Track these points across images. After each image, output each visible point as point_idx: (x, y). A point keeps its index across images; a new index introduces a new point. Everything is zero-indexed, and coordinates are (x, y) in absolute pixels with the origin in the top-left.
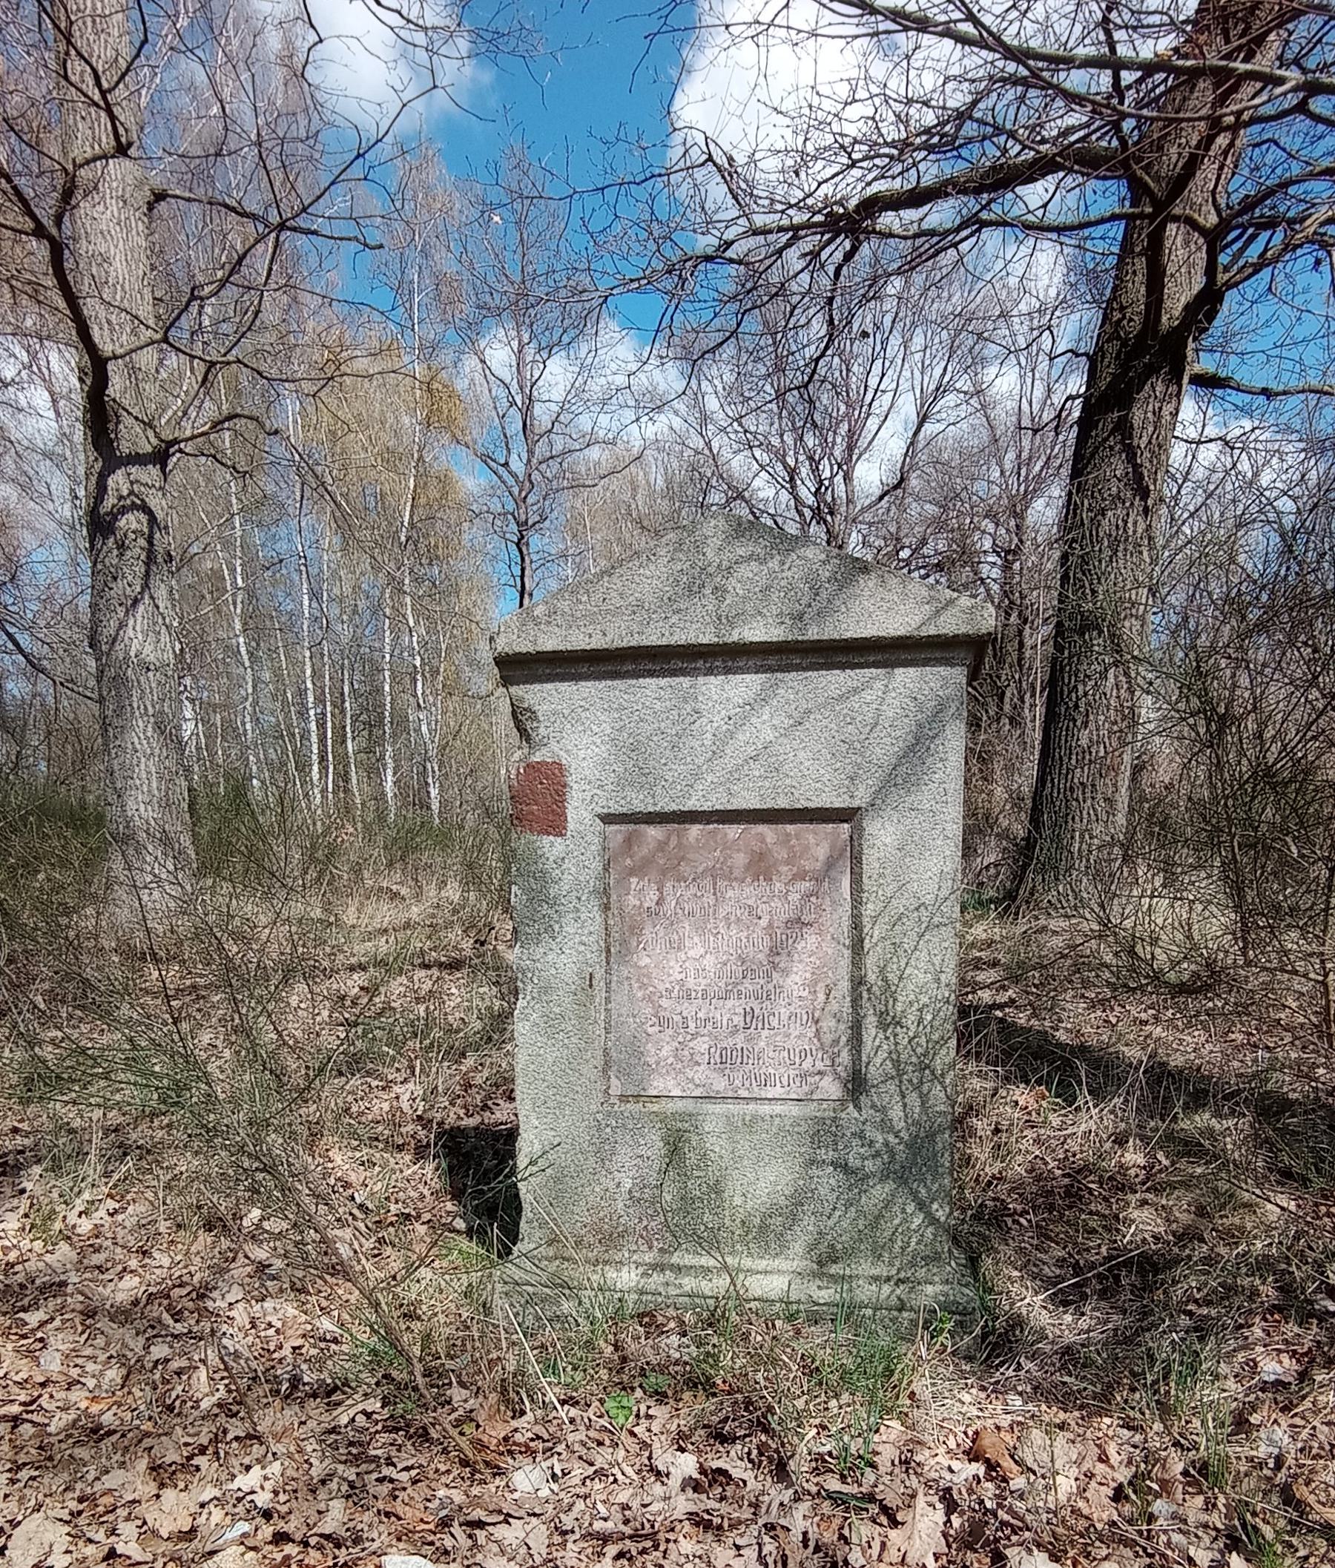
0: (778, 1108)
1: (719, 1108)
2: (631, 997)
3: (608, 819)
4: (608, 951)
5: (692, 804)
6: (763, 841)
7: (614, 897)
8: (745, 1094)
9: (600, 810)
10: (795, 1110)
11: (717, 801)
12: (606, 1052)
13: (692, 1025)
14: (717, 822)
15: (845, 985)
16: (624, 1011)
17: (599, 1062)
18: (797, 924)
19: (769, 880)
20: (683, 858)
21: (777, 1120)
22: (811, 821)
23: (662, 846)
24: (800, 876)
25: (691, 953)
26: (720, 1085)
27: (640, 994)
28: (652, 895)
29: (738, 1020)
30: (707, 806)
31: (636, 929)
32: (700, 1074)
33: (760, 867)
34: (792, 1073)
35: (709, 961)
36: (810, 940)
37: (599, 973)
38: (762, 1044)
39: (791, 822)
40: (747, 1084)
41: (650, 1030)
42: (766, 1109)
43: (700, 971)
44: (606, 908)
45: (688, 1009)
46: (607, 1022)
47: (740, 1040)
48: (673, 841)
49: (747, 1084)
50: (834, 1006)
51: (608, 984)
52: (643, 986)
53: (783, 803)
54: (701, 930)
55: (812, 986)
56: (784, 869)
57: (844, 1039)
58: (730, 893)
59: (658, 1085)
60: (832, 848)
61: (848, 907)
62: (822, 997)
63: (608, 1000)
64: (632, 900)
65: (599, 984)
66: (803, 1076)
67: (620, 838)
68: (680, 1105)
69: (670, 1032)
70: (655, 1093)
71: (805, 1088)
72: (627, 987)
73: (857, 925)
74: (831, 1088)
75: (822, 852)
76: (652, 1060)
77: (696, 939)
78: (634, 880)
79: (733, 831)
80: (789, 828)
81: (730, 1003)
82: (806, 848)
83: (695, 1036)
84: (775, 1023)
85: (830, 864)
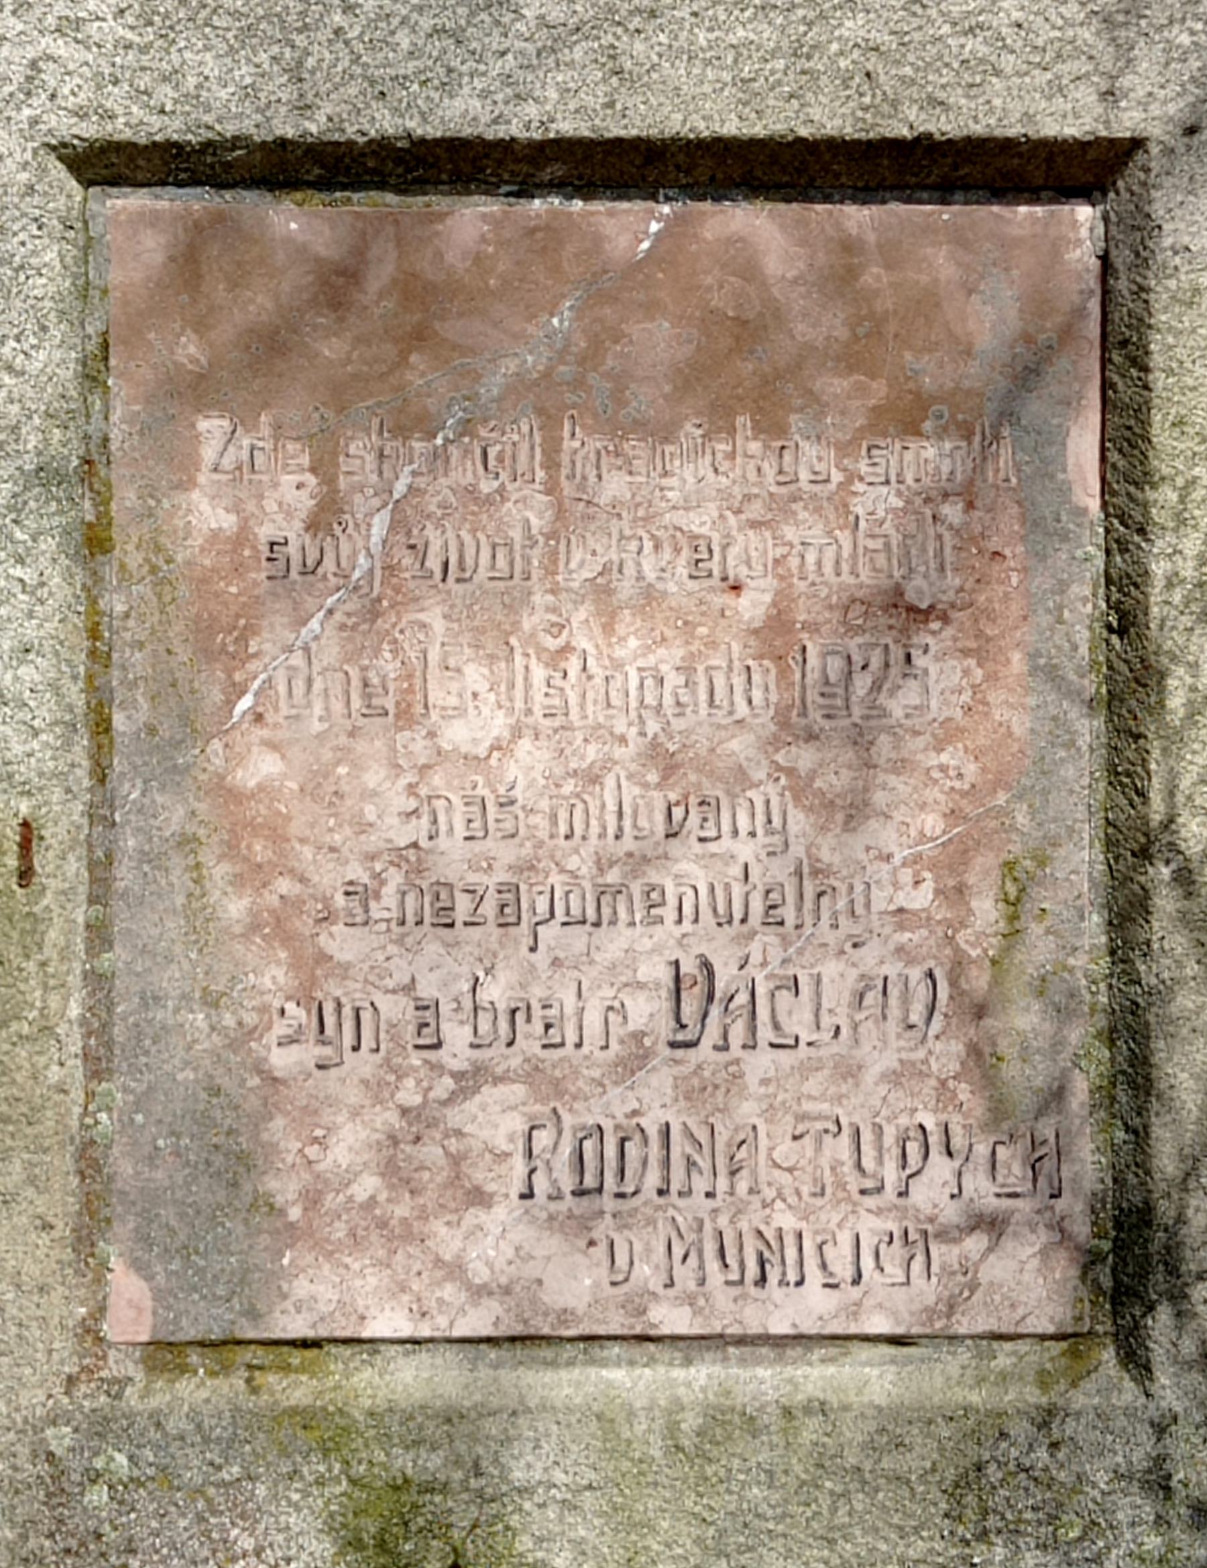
0: (814, 1376)
1: (565, 1384)
2: (199, 919)
3: (102, 164)
4: (101, 726)
5: (463, 112)
6: (750, 271)
7: (126, 498)
8: (672, 1318)
9: (65, 127)
10: (873, 1380)
11: (566, 105)
12: (89, 1159)
13: (457, 1036)
14: (559, 186)
15: (1081, 863)
16: (170, 980)
17: (60, 1200)
18: (902, 613)
19: (772, 428)
20: (420, 337)
21: (810, 1430)
22: (944, 192)
23: (337, 285)
24: (906, 417)
25: (456, 734)
26: (575, 1287)
27: (236, 908)
28: (290, 493)
29: (646, 1011)
30: (521, 123)
31: (224, 641)
32: (494, 1240)
33: (741, 379)
34: (871, 1227)
35: (528, 765)
36: (941, 676)
37: (63, 820)
38: (748, 1110)
39: (866, 193)
40: (685, 1276)
41: (281, 1060)
42: (763, 1381)
43: (493, 812)
44: (94, 542)
45: (438, 970)
46: (98, 1026)
47: (656, 1099)
48: (381, 272)
49: (685, 1276)
50: (1038, 949)
51: (100, 871)
52: (253, 876)
53: (829, 117)
54: (495, 637)
55: (950, 866)
56: (835, 385)
57: (1080, 1089)
58: (615, 486)
59: (311, 1296)
60: (1038, 303)
61: (1092, 548)
62: (986, 910)
63: (99, 935)
64: (207, 512)
65: (63, 869)
66: (919, 1239)
67: (153, 248)
68: (408, 1380)
69: (364, 1064)
70: (298, 1327)
71: (926, 1290)
72: (178, 876)
73: (1125, 619)
74: (1030, 1283)
75: (989, 320)
76: (285, 1189)
77: (475, 676)
78: (212, 427)
79: (632, 227)
80: (857, 217)
81: (614, 944)
82: (927, 304)
83: (470, 1080)
84: (798, 1022)
85: (1028, 370)
